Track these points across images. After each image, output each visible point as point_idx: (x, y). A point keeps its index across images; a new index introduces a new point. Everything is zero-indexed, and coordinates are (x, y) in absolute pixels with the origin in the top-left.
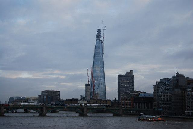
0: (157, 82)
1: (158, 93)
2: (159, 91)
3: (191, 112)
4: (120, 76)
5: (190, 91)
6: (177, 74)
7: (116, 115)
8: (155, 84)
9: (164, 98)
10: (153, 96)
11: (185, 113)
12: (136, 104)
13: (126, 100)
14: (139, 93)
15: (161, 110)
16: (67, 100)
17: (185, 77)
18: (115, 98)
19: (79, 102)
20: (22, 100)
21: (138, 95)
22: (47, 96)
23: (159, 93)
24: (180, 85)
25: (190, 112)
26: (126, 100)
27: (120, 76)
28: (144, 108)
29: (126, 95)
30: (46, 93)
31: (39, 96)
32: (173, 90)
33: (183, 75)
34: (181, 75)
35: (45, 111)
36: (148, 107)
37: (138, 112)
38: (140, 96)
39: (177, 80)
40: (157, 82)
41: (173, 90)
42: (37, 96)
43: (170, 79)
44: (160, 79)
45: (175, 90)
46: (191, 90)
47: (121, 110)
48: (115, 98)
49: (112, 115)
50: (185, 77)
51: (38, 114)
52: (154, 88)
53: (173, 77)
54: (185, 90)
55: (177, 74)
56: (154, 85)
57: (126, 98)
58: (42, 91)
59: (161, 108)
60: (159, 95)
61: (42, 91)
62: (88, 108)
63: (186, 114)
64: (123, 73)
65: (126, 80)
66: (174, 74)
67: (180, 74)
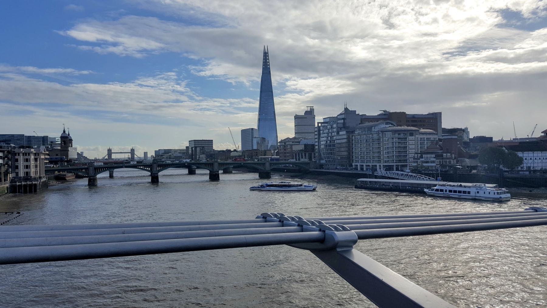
4: (297, 117)
5: (359, 135)
6: (346, 109)
11: (352, 166)
15: (323, 162)
20: (168, 153)
25: (358, 164)
27: (297, 117)
32: (338, 133)
40: (318, 123)
41: (338, 133)
45: (341, 133)
47: (267, 165)
53: (341, 114)
54: (353, 132)
55: (346, 109)
66: (341, 110)
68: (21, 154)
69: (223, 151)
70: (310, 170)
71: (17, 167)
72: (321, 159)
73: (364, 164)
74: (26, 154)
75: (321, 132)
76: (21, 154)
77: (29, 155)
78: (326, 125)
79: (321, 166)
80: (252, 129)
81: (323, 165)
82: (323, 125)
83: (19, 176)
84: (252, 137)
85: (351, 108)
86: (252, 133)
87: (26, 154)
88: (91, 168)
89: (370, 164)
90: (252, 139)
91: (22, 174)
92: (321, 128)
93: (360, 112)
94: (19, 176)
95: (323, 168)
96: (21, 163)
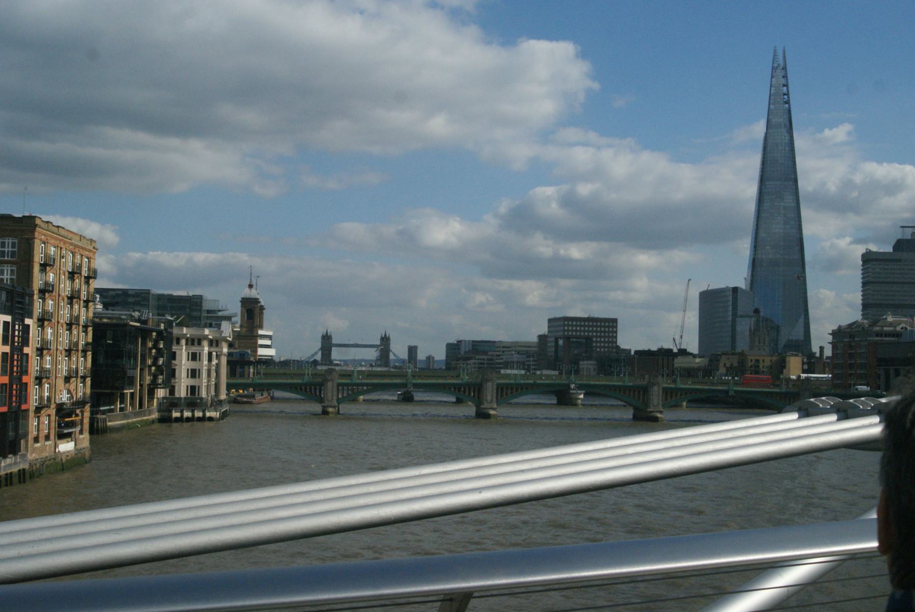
16: (636, 352)
22: (567, 338)
30: (565, 325)
31: (542, 338)
35: (489, 398)
42: (535, 339)
58: (550, 321)
61: (550, 321)
68: (183, 342)
69: (649, 353)
71: (172, 374)
74: (193, 340)
76: (183, 342)
77: (199, 343)
83: (177, 395)
87: (193, 340)
88: (329, 384)
91: (182, 392)
94: (177, 395)
96: (183, 363)
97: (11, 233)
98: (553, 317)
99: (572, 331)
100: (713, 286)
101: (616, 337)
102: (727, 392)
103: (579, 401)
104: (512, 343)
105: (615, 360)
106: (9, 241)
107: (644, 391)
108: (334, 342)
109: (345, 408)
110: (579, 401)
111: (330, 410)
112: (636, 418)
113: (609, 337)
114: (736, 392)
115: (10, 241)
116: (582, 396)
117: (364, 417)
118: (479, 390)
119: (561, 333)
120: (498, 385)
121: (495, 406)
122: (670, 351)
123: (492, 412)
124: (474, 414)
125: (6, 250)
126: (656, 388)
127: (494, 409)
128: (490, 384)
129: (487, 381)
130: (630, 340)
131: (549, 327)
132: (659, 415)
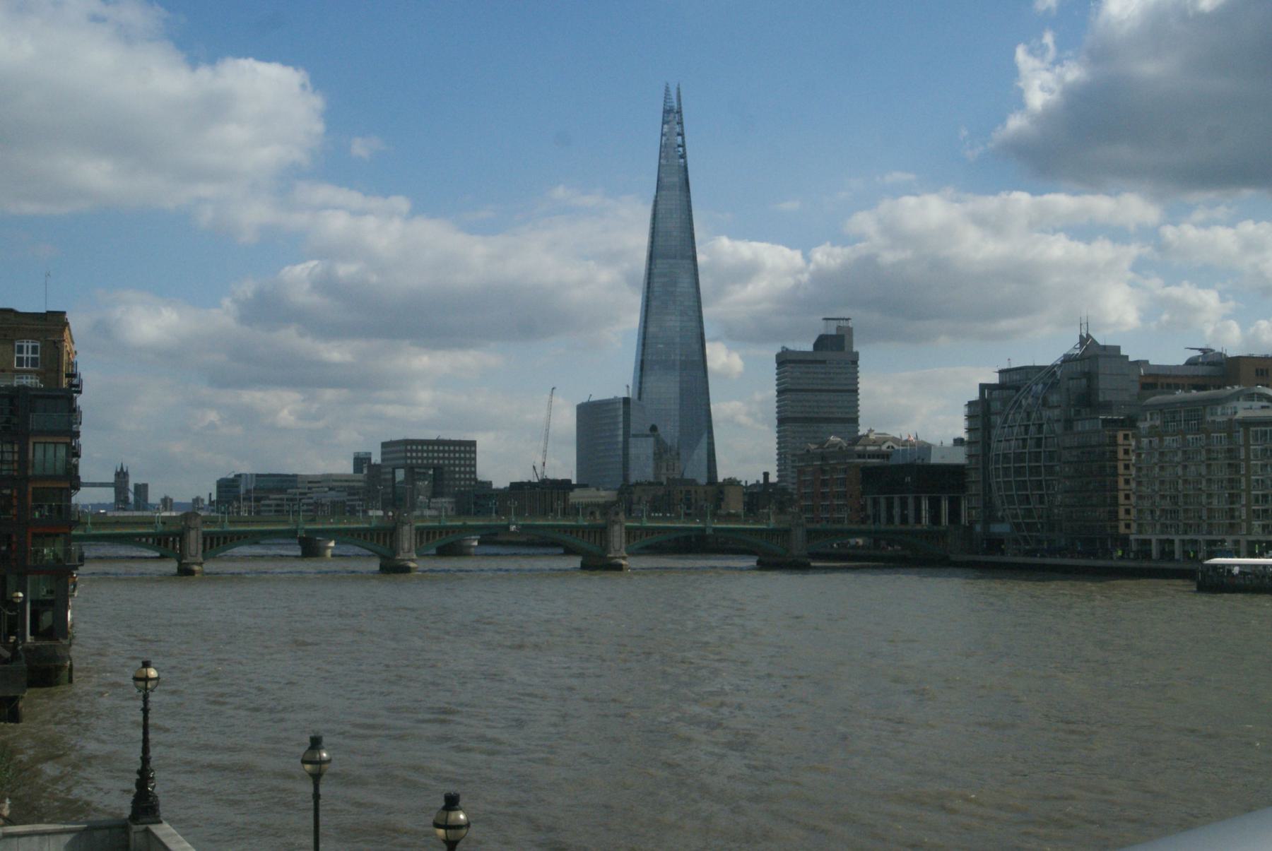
0: (983, 387)
1: (987, 445)
2: (996, 433)
3: (1161, 542)
6: (1085, 340)
7: (770, 563)
8: (975, 395)
9: (1019, 471)
10: (959, 457)
12: (876, 503)
13: (824, 483)
14: (890, 444)
16: (516, 487)
17: (1131, 359)
18: (766, 475)
19: (576, 497)
21: (886, 456)
23: (994, 445)
24: (1101, 399)
26: (824, 483)
28: (918, 519)
29: (823, 458)
32: (1068, 424)
33: (1118, 348)
34: (1105, 347)
35: (406, 546)
36: (935, 518)
37: (883, 543)
38: (892, 462)
39: (1090, 376)
40: (983, 387)
41: (1068, 424)
43: (1049, 371)
44: (1001, 372)
45: (1078, 426)
46: (1158, 423)
48: (766, 475)
49: (752, 562)
50: (1131, 359)
51: (375, 565)
52: (970, 417)
53: (1067, 359)
56: (970, 404)
57: (823, 472)
59: (1002, 520)
60: (992, 454)
62: (627, 528)
63: (1134, 547)
64: (806, 345)
65: (817, 377)
66: (1068, 344)
67: (1101, 343)
70: (953, 557)
72: (990, 518)
73: (1177, 539)
75: (998, 420)
78: (1006, 393)
79: (995, 544)
80: (626, 401)
81: (1002, 541)
82: (996, 393)
84: (627, 434)
85: (1103, 338)
86: (627, 414)
88: (193, 534)
89: (1200, 538)
90: (626, 443)
92: (996, 406)
93: (1133, 353)
95: (1003, 552)
97: (31, 334)
98: (388, 440)
99: (417, 458)
100: (597, 397)
101: (475, 466)
102: (703, 530)
103: (472, 550)
104: (323, 475)
105: (480, 497)
106: (28, 344)
107: (602, 532)
108: (82, 480)
109: (210, 566)
110: (472, 550)
111: (196, 568)
112: (584, 567)
113: (465, 466)
114: (715, 529)
115: (30, 345)
116: (476, 543)
117: (237, 577)
118: (391, 535)
119: (402, 462)
120: (418, 529)
121: (415, 557)
122: (569, 481)
123: (412, 565)
124: (377, 568)
125: (25, 355)
126: (617, 527)
127: (413, 560)
128: (406, 528)
129: (403, 523)
130: (499, 467)
131: (383, 453)
132: (623, 562)
